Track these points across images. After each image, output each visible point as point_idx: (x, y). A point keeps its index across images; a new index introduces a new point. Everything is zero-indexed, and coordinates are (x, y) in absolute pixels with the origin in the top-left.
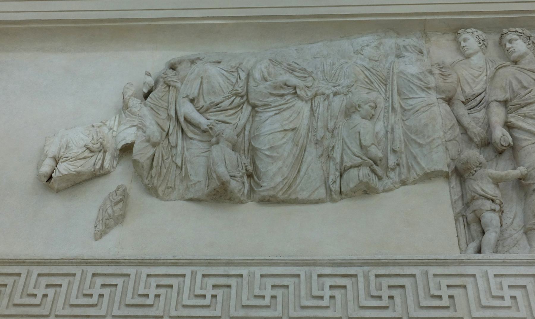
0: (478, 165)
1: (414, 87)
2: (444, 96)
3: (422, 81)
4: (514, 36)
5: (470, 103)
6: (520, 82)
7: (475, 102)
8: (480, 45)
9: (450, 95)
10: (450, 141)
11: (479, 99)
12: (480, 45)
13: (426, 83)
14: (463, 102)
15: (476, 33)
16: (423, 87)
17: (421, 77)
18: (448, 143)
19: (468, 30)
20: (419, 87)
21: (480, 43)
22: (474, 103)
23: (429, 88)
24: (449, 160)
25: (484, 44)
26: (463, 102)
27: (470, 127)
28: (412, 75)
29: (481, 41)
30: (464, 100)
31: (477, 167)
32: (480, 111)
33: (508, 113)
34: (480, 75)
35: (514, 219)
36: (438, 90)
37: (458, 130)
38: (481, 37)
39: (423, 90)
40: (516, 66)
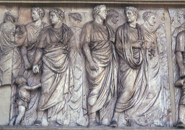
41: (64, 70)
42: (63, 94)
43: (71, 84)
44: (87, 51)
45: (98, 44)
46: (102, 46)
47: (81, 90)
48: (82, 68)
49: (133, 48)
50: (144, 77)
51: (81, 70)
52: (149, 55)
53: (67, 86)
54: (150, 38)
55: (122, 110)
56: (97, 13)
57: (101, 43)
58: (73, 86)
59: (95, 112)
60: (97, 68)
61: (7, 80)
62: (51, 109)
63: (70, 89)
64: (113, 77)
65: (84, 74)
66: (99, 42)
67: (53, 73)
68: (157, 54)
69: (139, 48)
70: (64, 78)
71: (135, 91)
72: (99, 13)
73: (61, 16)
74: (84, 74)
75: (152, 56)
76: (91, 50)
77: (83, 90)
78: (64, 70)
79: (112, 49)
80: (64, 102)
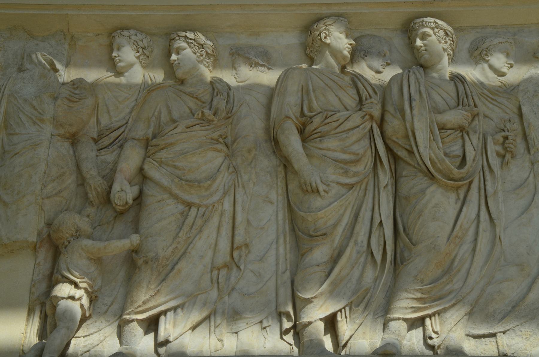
0: (74, 232)
1: (23, 118)
2: (62, 131)
3: (36, 110)
4: (184, 45)
5: (102, 141)
6: (170, 112)
7: (113, 140)
8: (138, 54)
9: (73, 130)
10: (48, 198)
11: (114, 135)
12: (138, 54)
13: (41, 114)
14: (94, 139)
15: (133, 38)
16: (34, 119)
17: (35, 103)
18: (46, 201)
19: (125, 33)
20: (30, 118)
21: (138, 52)
22: (106, 141)
23: (42, 121)
24: (42, 224)
25: (144, 54)
26: (94, 139)
27: (88, 176)
28: (25, 100)
29: (140, 50)
30: (95, 136)
31: (72, 236)
32: (113, 152)
33: (147, 156)
34: (128, 99)
35: (110, 306)
36: (56, 122)
37: (70, 180)
38: (140, 43)
39: (35, 123)
40: (181, 88)
41: (216, 198)
42: (213, 268)
43: (239, 239)
44: (293, 142)
45: (326, 118)
46: (340, 125)
47: (271, 259)
48: (273, 196)
49: (442, 128)
50: (484, 214)
51: (272, 203)
52: (498, 154)
53: (224, 245)
54: (496, 109)
55: (415, 312)
56: (321, 39)
57: (335, 118)
58: (247, 245)
59: (321, 320)
60: (325, 187)
61: (28, 225)
62: (169, 314)
63: (236, 254)
64: (376, 216)
65: (243, 84)
66: (327, 114)
67: (181, 207)
68: (526, 152)
69: (461, 129)
70: (215, 221)
71: (455, 256)
72: (325, 37)
73: (207, 53)
74: (243, 84)
75: (508, 156)
76: (304, 140)
77: (277, 259)
78: (216, 198)
79: (372, 138)
80: (214, 294)
